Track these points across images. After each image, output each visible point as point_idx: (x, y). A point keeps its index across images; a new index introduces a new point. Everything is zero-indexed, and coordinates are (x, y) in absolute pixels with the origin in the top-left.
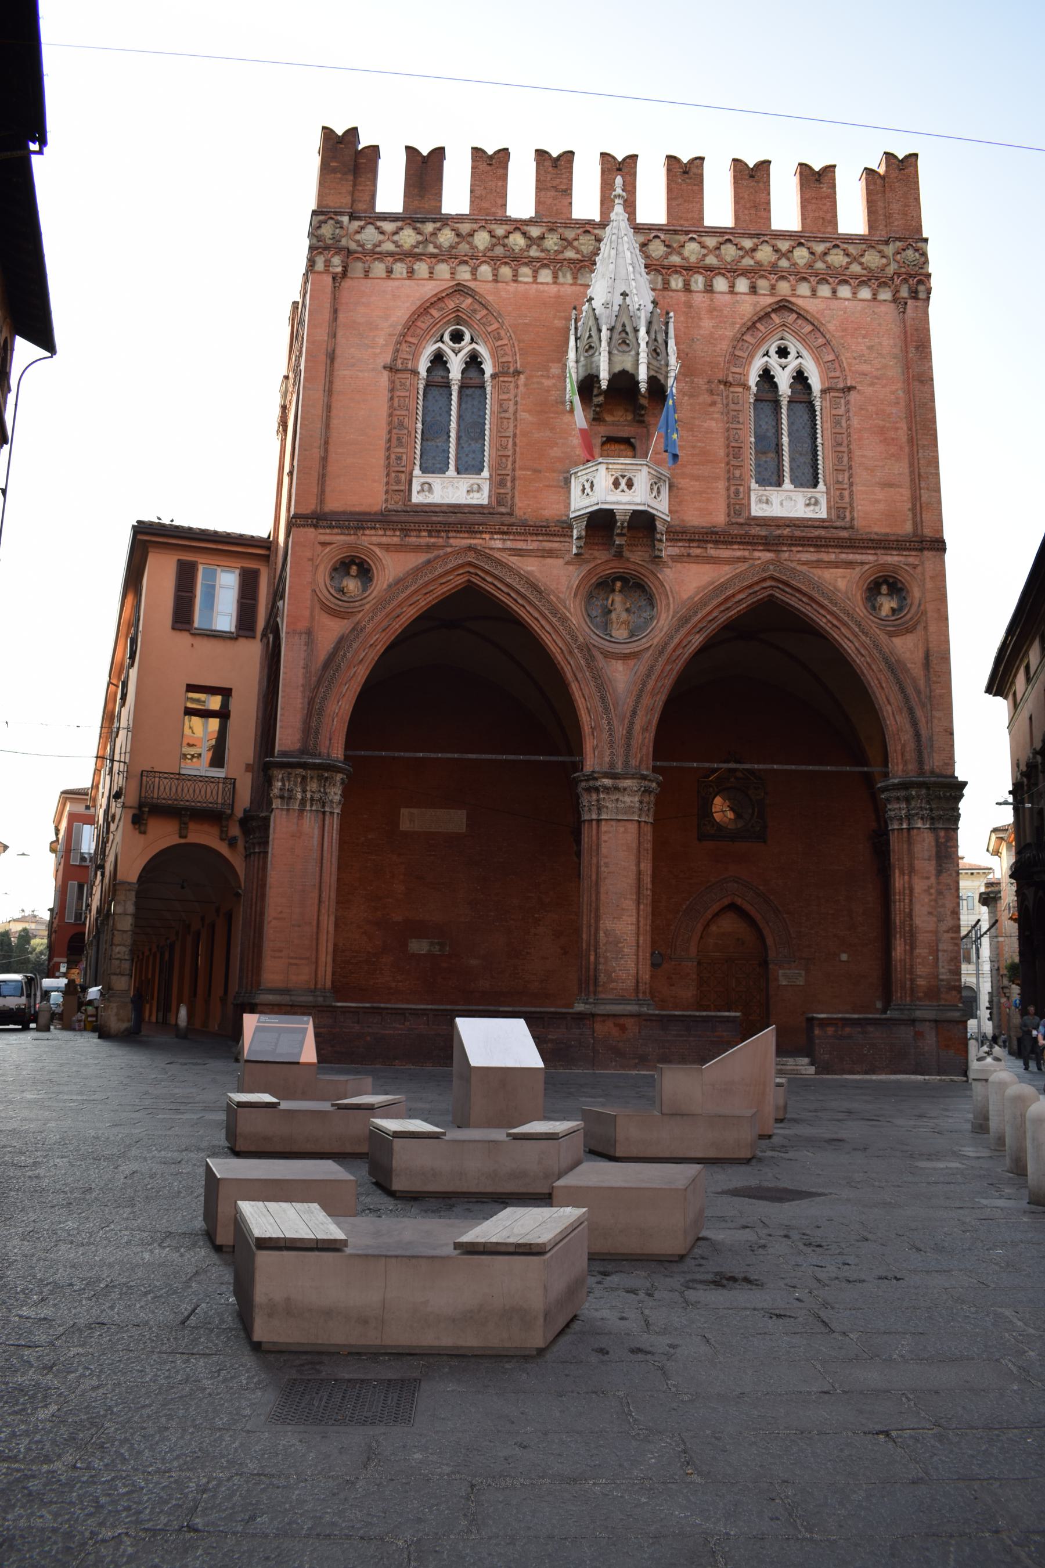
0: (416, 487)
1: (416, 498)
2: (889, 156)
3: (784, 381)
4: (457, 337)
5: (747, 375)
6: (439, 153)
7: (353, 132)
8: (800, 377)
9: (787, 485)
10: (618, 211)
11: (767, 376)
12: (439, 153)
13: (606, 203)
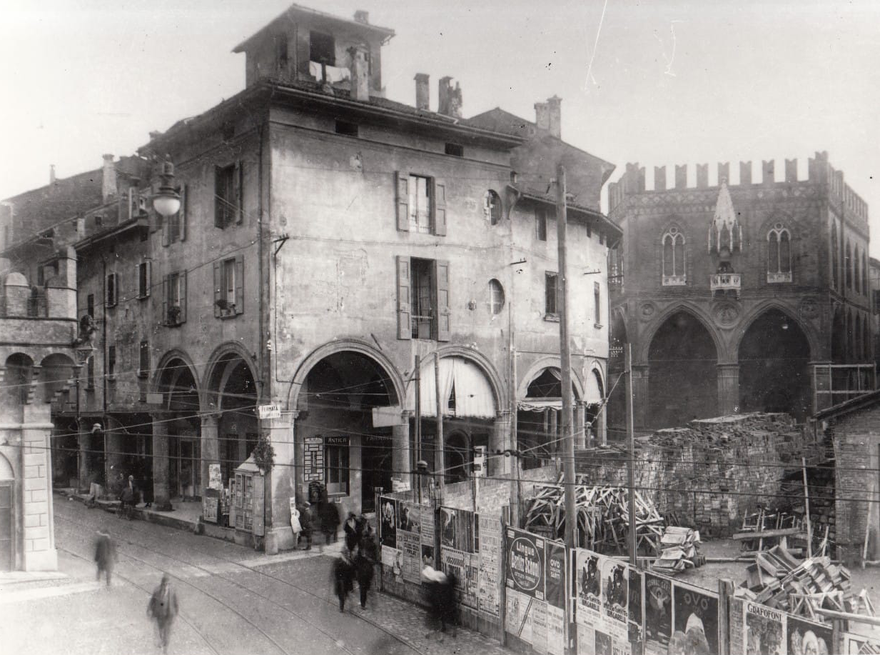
0: (663, 280)
1: (664, 284)
2: (817, 154)
3: (779, 236)
4: (673, 230)
5: (765, 237)
6: (664, 168)
7: (637, 164)
8: (784, 233)
9: (780, 272)
10: (724, 186)
11: (773, 234)
12: (664, 168)
13: (720, 182)
